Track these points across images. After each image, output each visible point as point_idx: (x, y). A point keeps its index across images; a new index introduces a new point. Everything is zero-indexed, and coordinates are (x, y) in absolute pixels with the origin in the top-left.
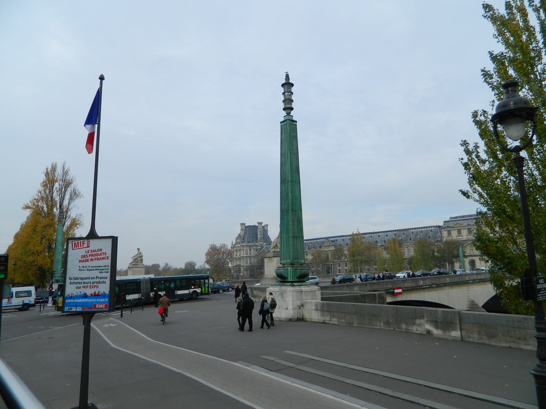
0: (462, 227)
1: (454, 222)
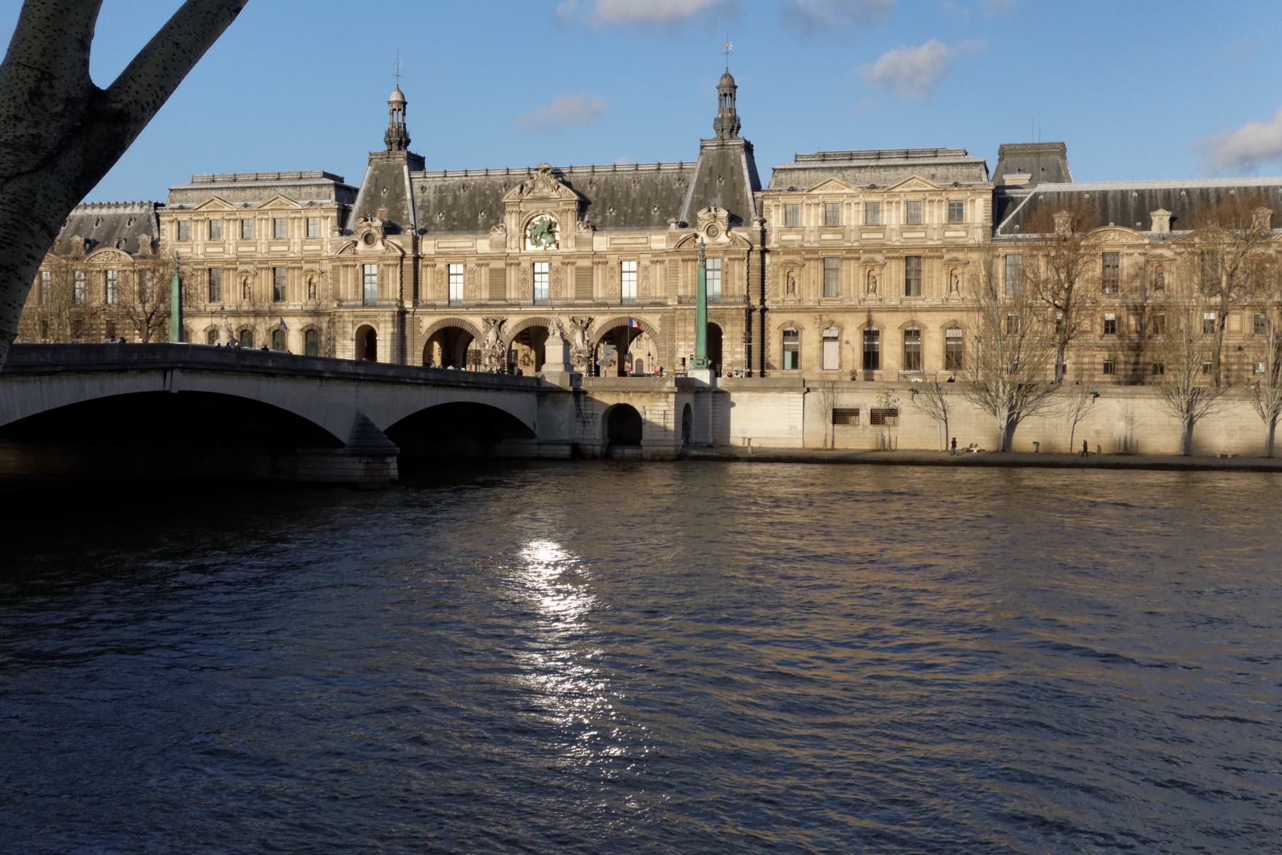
1: (203, 192)
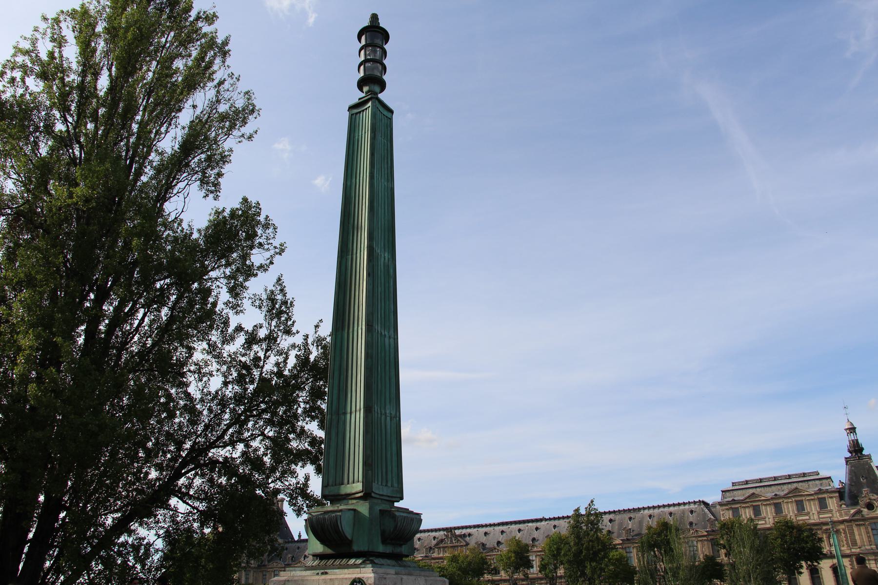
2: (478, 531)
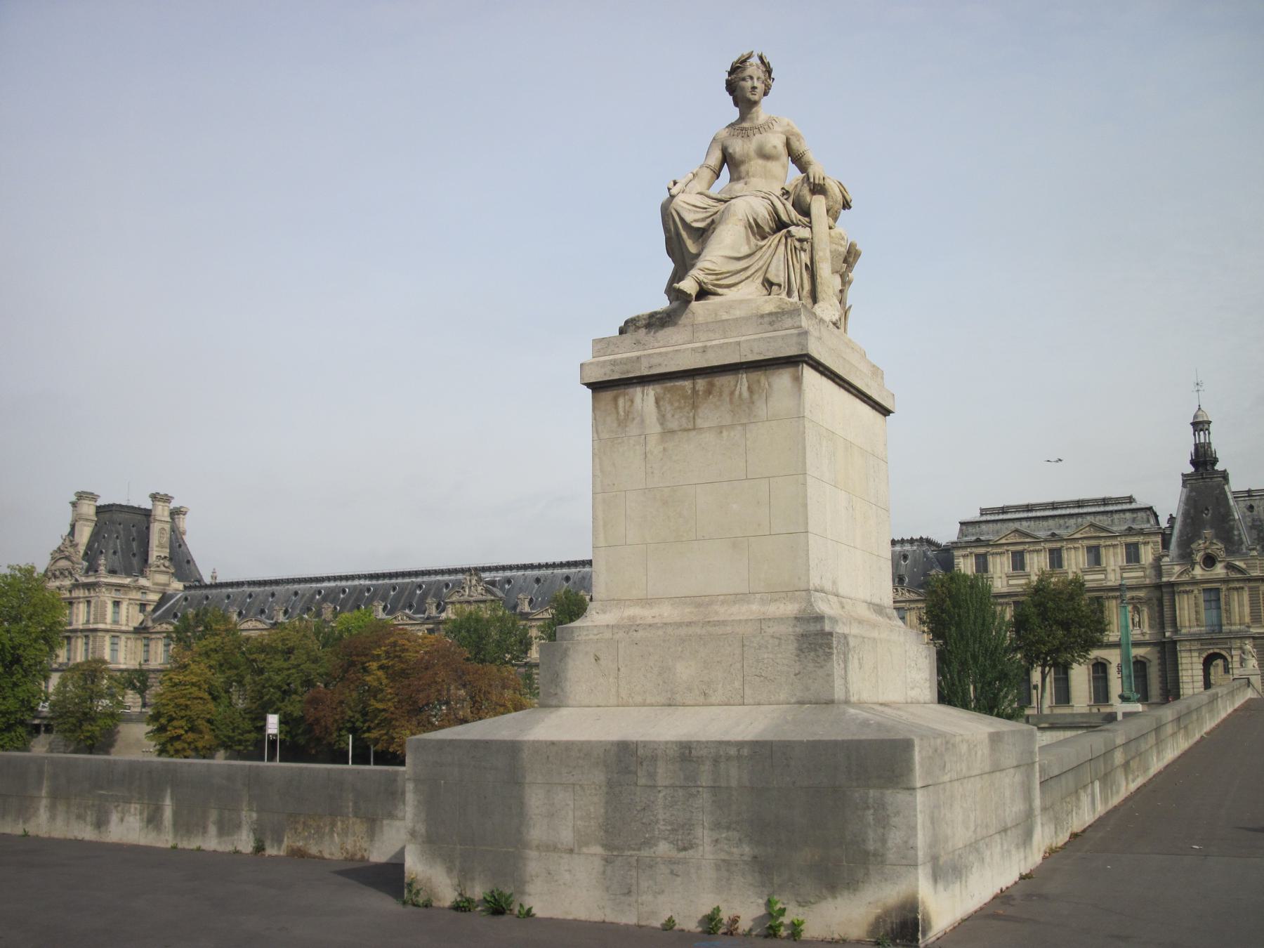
0: (1026, 547)
2: (523, 575)
